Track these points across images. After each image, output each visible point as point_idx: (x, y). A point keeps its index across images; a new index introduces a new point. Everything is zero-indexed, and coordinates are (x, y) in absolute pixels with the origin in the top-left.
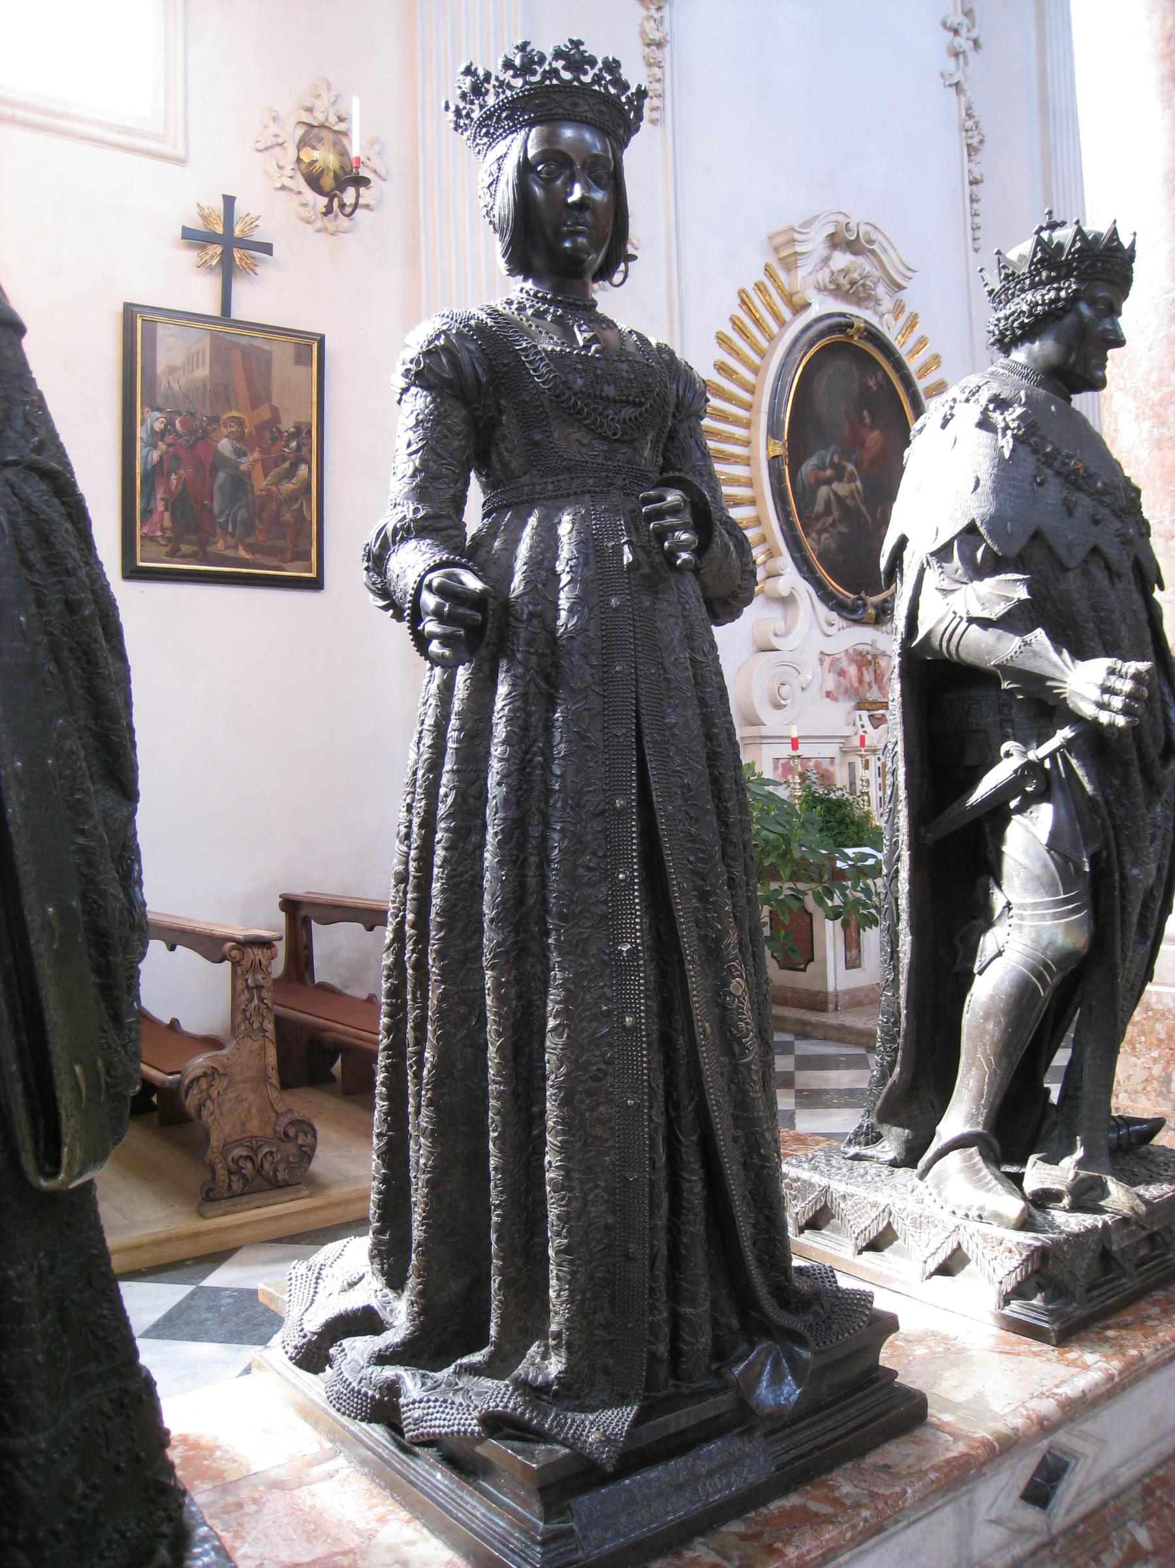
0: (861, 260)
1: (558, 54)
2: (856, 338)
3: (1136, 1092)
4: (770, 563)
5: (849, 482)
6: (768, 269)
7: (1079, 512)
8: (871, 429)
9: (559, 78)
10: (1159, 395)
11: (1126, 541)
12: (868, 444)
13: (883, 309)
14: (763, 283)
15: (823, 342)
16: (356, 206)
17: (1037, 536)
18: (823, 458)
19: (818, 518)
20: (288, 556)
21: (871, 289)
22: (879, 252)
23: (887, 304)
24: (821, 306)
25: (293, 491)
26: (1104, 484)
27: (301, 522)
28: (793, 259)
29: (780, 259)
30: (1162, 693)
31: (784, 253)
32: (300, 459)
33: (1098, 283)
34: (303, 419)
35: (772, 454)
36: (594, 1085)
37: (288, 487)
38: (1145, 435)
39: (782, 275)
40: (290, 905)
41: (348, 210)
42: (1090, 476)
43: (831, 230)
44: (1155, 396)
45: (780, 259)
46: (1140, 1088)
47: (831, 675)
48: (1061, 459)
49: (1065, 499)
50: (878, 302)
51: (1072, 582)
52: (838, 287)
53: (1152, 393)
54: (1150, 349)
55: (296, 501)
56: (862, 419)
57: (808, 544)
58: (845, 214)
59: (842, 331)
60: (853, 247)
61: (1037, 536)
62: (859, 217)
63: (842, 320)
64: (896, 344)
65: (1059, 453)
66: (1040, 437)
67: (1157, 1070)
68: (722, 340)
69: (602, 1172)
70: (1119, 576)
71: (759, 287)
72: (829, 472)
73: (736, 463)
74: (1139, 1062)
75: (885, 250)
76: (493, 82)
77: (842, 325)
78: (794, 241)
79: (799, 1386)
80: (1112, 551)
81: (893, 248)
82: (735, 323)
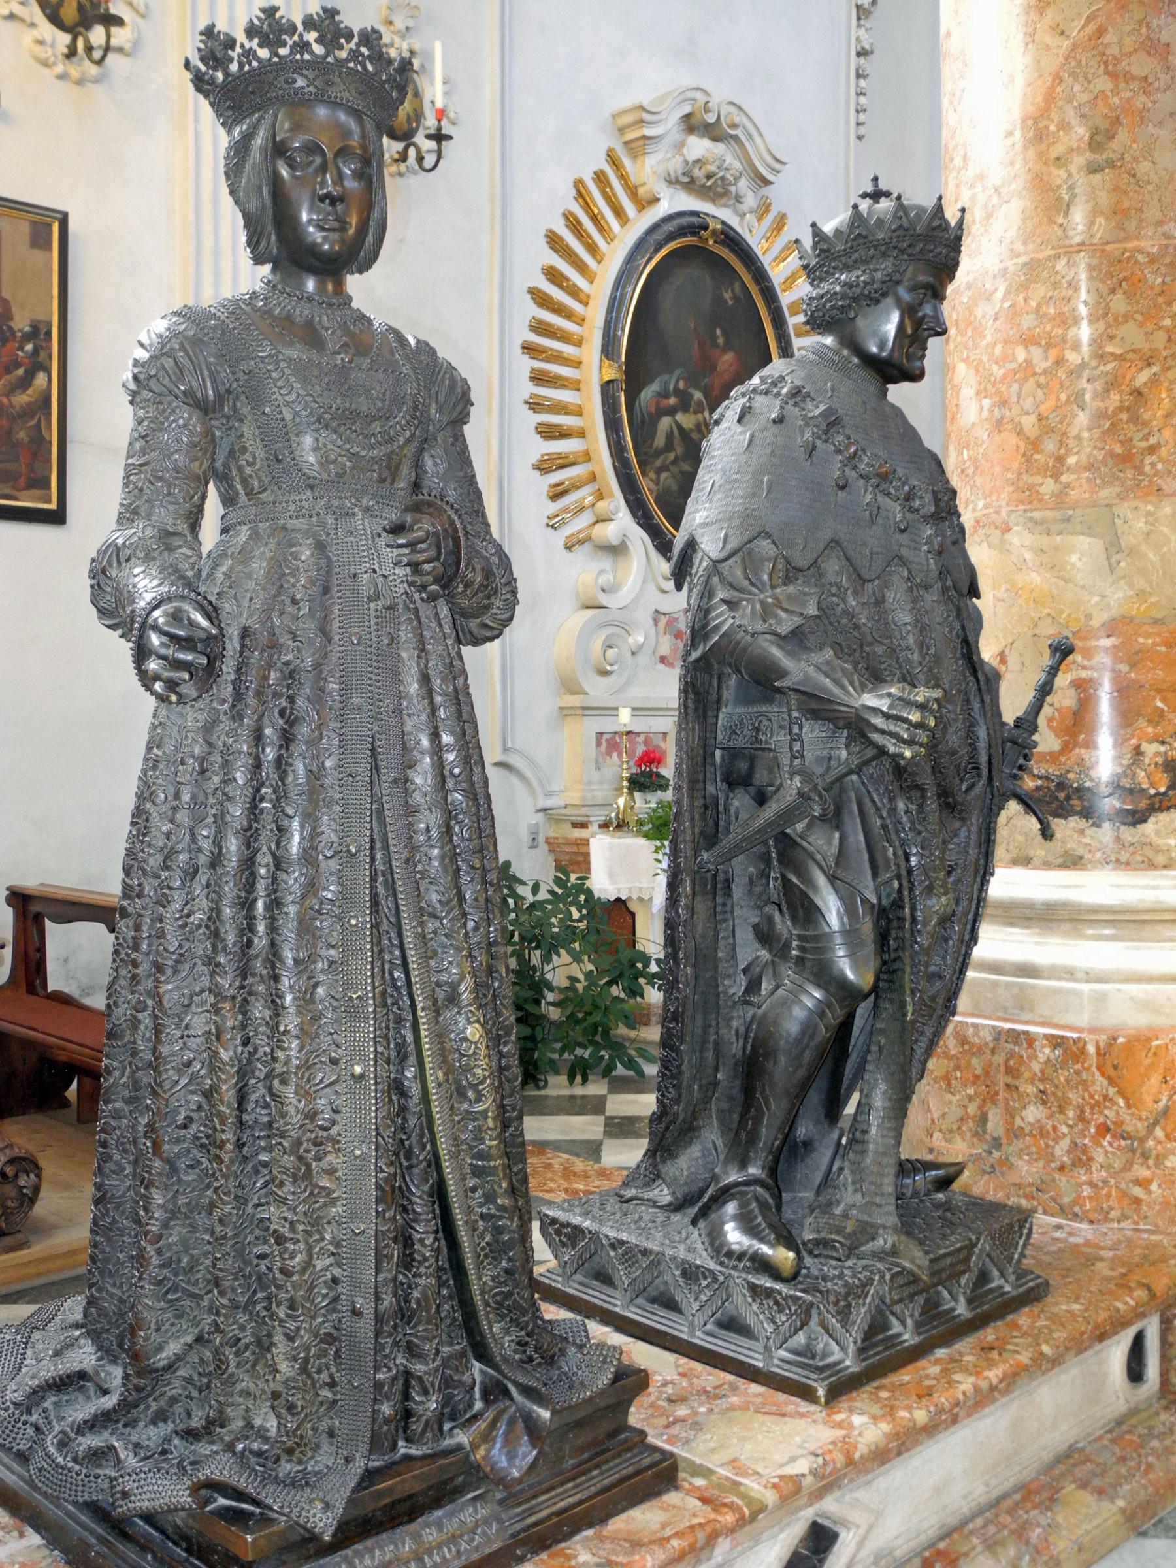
0: (720, 148)
1: (309, 23)
2: (711, 242)
3: (951, 1131)
4: (601, 505)
5: (695, 413)
8: (724, 352)
9: (311, 52)
10: (1002, 372)
12: (720, 367)
13: (744, 208)
14: (602, 172)
15: (673, 245)
16: (107, 49)
18: (666, 383)
19: (658, 453)
20: (22, 481)
21: (730, 184)
22: (743, 138)
23: (750, 201)
24: (673, 202)
25: (29, 404)
27: (39, 443)
28: (641, 143)
29: (626, 143)
31: (629, 136)
32: (38, 365)
34: (42, 317)
35: (606, 378)
36: (321, 1133)
37: (22, 399)
38: (985, 414)
40: (20, 899)
41: (97, 55)
43: (687, 109)
44: (998, 372)
46: (955, 1127)
47: (668, 637)
50: (738, 199)
52: (693, 180)
53: (995, 368)
54: (996, 319)
55: (33, 417)
56: (714, 338)
57: (645, 484)
58: (704, 91)
59: (694, 234)
60: (713, 132)
62: (721, 94)
63: (694, 219)
64: (758, 251)
67: (972, 1109)
68: (554, 241)
69: (329, 1223)
72: (672, 401)
73: (563, 387)
74: (954, 1099)
75: (750, 136)
76: (238, 49)
77: (693, 225)
78: (642, 121)
79: (534, 1447)
81: (761, 135)
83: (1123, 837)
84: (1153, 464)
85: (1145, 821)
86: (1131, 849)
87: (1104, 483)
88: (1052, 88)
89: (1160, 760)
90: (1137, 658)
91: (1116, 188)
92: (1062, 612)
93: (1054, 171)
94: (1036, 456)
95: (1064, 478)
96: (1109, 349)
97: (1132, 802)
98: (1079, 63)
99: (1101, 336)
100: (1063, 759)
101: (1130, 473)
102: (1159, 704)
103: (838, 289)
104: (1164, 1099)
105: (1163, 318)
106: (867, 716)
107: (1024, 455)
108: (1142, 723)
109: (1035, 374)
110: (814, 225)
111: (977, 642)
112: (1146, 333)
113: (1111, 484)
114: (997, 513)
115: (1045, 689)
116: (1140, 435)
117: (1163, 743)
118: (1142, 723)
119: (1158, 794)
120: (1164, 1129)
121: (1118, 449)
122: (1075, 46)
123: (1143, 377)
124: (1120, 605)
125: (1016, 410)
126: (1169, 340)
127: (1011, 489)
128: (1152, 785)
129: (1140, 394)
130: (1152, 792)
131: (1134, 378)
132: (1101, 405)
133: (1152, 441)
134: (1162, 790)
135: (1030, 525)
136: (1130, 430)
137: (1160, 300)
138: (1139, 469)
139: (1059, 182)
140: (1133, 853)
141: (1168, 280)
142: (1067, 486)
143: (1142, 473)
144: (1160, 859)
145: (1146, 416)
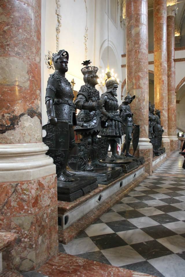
84: (8, 49)
85: (5, 132)
86: (2, 139)
89: (8, 118)
90: (3, 93)
102: (8, 105)
104: (6, 199)
108: (4, 109)
116: (5, 41)
117: (9, 114)
118: (4, 109)
119: (8, 126)
120: (6, 207)
126: (13, 21)
130: (7, 125)
131: (4, 28)
133: (8, 43)
134: (9, 125)
138: (5, 49)
143: (5, 50)
145: (7, 37)
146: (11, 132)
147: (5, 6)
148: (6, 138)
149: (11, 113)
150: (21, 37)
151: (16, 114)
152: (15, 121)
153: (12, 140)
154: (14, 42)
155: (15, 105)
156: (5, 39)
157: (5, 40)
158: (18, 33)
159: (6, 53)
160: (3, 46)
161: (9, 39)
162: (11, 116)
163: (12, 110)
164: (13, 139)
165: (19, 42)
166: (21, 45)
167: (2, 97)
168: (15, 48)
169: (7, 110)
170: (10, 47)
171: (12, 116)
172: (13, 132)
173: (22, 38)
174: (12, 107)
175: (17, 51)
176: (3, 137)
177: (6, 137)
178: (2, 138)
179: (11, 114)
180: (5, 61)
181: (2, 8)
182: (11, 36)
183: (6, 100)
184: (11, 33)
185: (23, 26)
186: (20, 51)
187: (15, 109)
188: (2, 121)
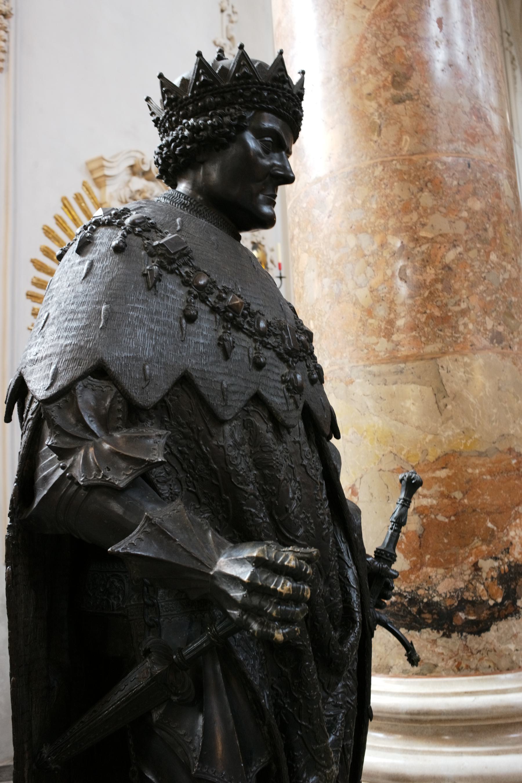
6: (84, 184)
7: (238, 353)
11: (294, 389)
14: (80, 194)
17: (185, 381)
26: (268, 324)
28: (103, 179)
30: (339, 550)
33: (266, 114)
38: (326, 290)
39: (95, 190)
42: (252, 315)
43: (131, 162)
45: (95, 180)
48: (216, 293)
49: (221, 339)
51: (230, 436)
54: (329, 216)
58: (142, 154)
61: (185, 381)
65: (215, 287)
66: (193, 267)
70: (288, 428)
71: (78, 198)
80: (277, 400)
82: (59, 220)
83: (470, 645)
84: (465, 325)
85: (488, 629)
87: (428, 340)
88: (360, 45)
89: (495, 574)
91: (416, 114)
92: (402, 449)
93: (367, 103)
94: (371, 321)
95: (395, 337)
96: (423, 234)
97: (475, 613)
98: (379, 28)
99: (415, 224)
100: (413, 577)
101: (448, 332)
102: (490, 525)
103: (186, 133)
105: (460, 211)
106: (224, 587)
107: (361, 320)
108: (477, 542)
109: (365, 256)
110: (161, 76)
111: (339, 480)
112: (450, 222)
113: (434, 341)
114: (342, 369)
115: (400, 522)
116: (453, 301)
117: (496, 559)
118: (477, 542)
119: (496, 604)
121: (437, 313)
122: (374, 16)
123: (451, 256)
124: (450, 441)
125: (351, 285)
126: (468, 227)
127: (352, 349)
128: (491, 597)
129: (450, 269)
130: (491, 602)
131: (443, 256)
132: (420, 278)
133: (463, 306)
135: (369, 377)
136: (445, 298)
137: (458, 197)
138: (455, 328)
139: (371, 110)
140: (481, 659)
141: (461, 183)
142: (398, 344)
144: (504, 663)
146: (510, 627)
147: (441, 183)
148: (495, 651)
149: (499, 556)
150: (498, 278)
151: (517, 555)
152: (517, 584)
153: (514, 658)
154: (480, 299)
155: (510, 524)
156: (452, 294)
157: (451, 297)
158: (489, 267)
159: (462, 340)
160: (450, 317)
161: (464, 292)
162: (503, 564)
163: (503, 541)
164: (517, 650)
165: (494, 296)
166: (501, 307)
167: (466, 501)
168: (487, 318)
169: (488, 545)
170: (469, 319)
171: (506, 567)
172: (515, 626)
173: (501, 281)
174: (502, 531)
175: (492, 331)
176: (481, 647)
177: (492, 647)
178: (479, 651)
179: (502, 560)
180: (463, 370)
181: (430, 191)
182: (469, 281)
183: (478, 510)
184: (468, 270)
185: (498, 241)
186: (501, 329)
187: (513, 538)
188: (475, 588)
